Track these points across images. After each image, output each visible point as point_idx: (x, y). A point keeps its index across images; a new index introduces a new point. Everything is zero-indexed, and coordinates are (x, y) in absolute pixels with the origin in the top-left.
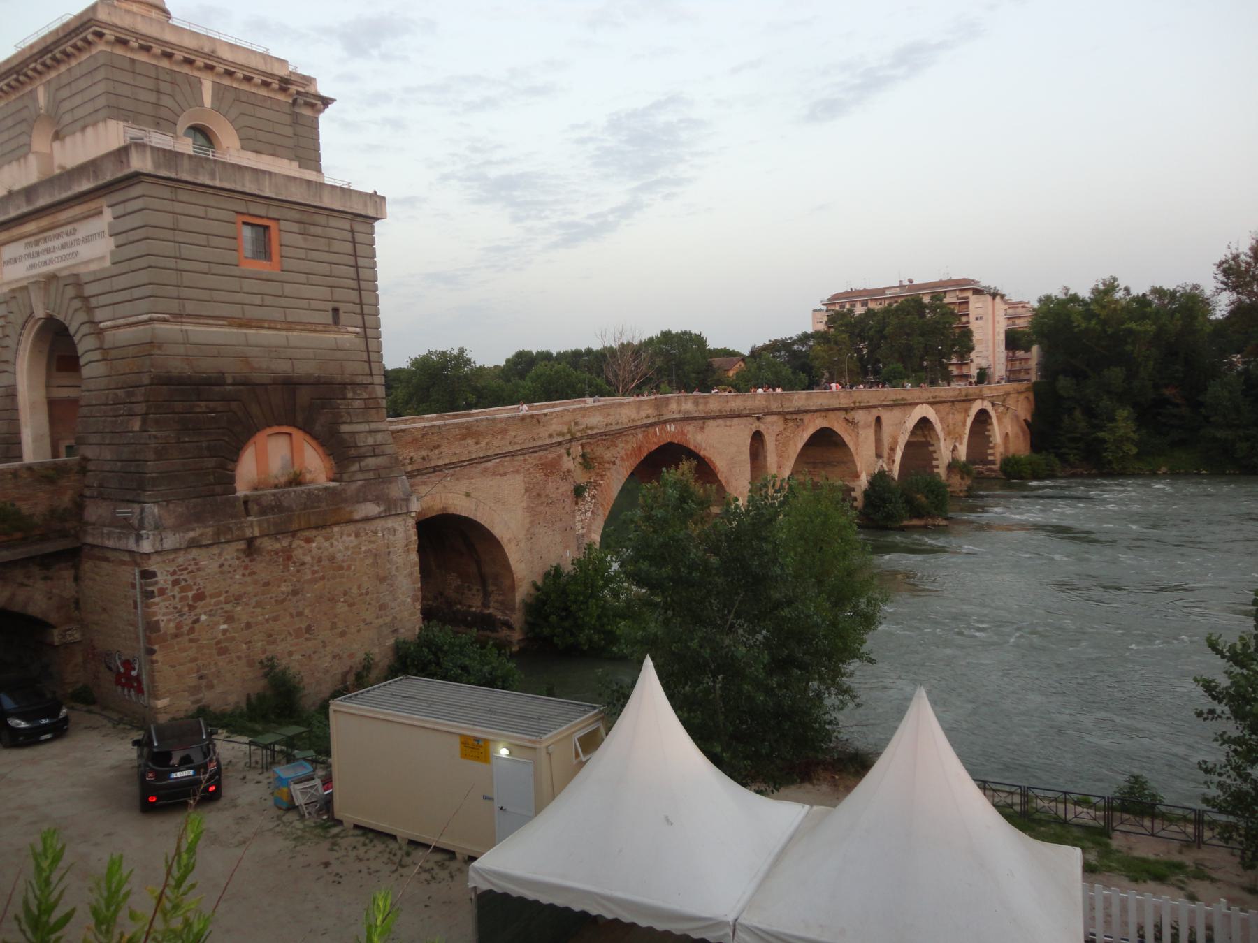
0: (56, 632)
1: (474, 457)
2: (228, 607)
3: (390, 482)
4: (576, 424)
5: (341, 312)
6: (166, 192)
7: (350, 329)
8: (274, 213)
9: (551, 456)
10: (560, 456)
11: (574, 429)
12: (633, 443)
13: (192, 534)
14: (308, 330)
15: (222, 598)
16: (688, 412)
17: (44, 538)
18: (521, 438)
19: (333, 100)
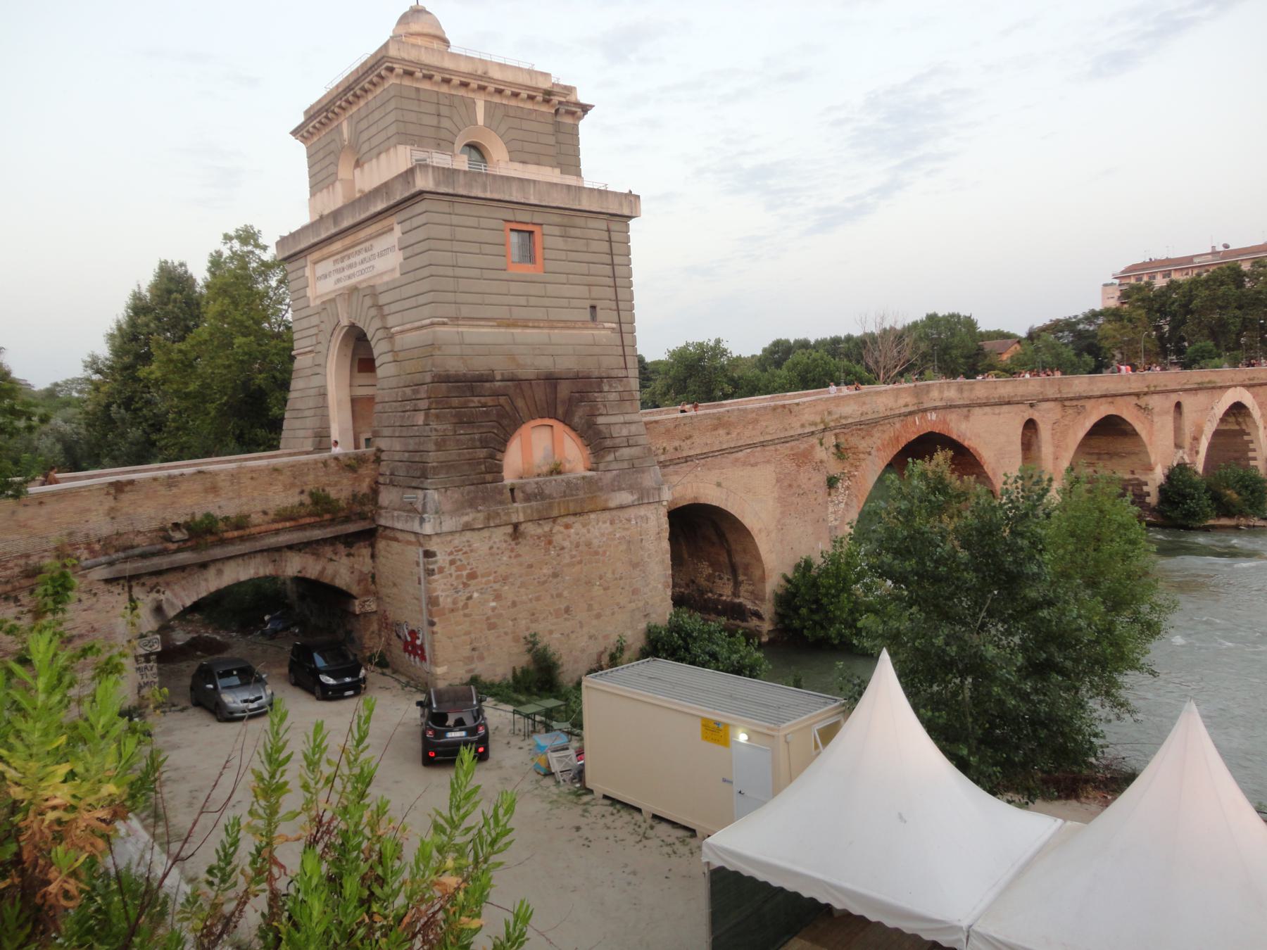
0: (357, 602)
1: (724, 447)
2: (496, 586)
3: (643, 472)
4: (830, 413)
5: (598, 309)
6: (443, 206)
7: (607, 325)
8: (538, 218)
9: (803, 446)
10: (812, 447)
11: (828, 419)
12: (890, 432)
13: (466, 519)
14: (569, 328)
15: (491, 578)
16: (952, 400)
17: (347, 520)
18: (772, 427)
19: (592, 106)
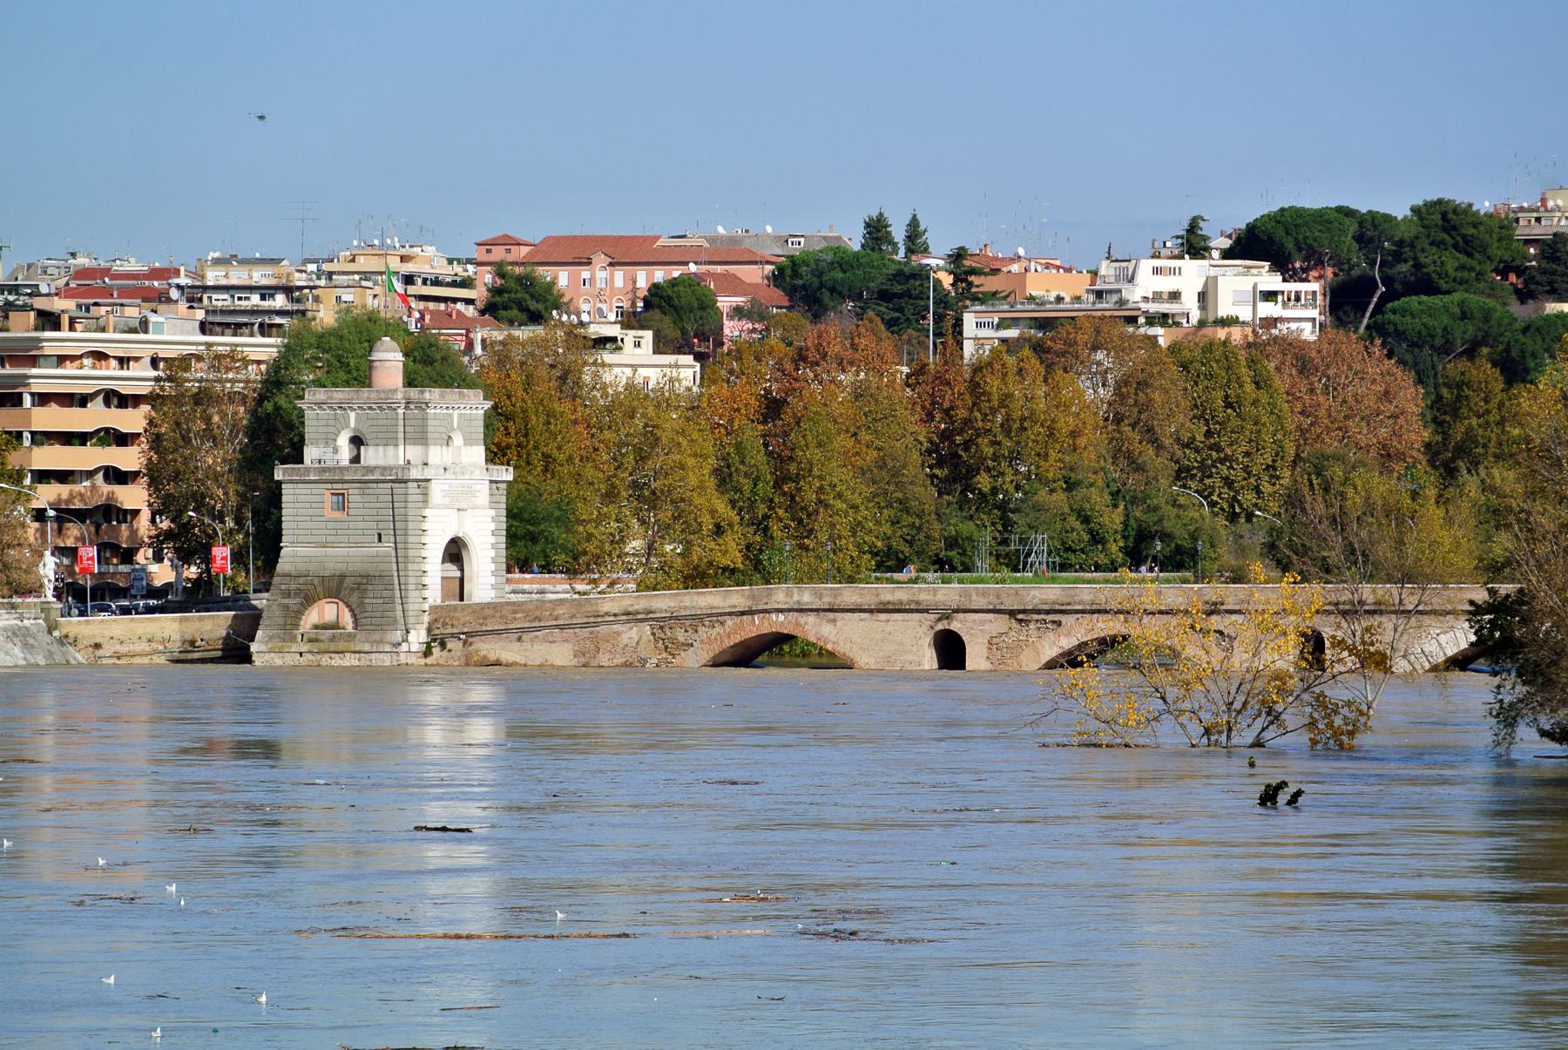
8: (346, 486)
